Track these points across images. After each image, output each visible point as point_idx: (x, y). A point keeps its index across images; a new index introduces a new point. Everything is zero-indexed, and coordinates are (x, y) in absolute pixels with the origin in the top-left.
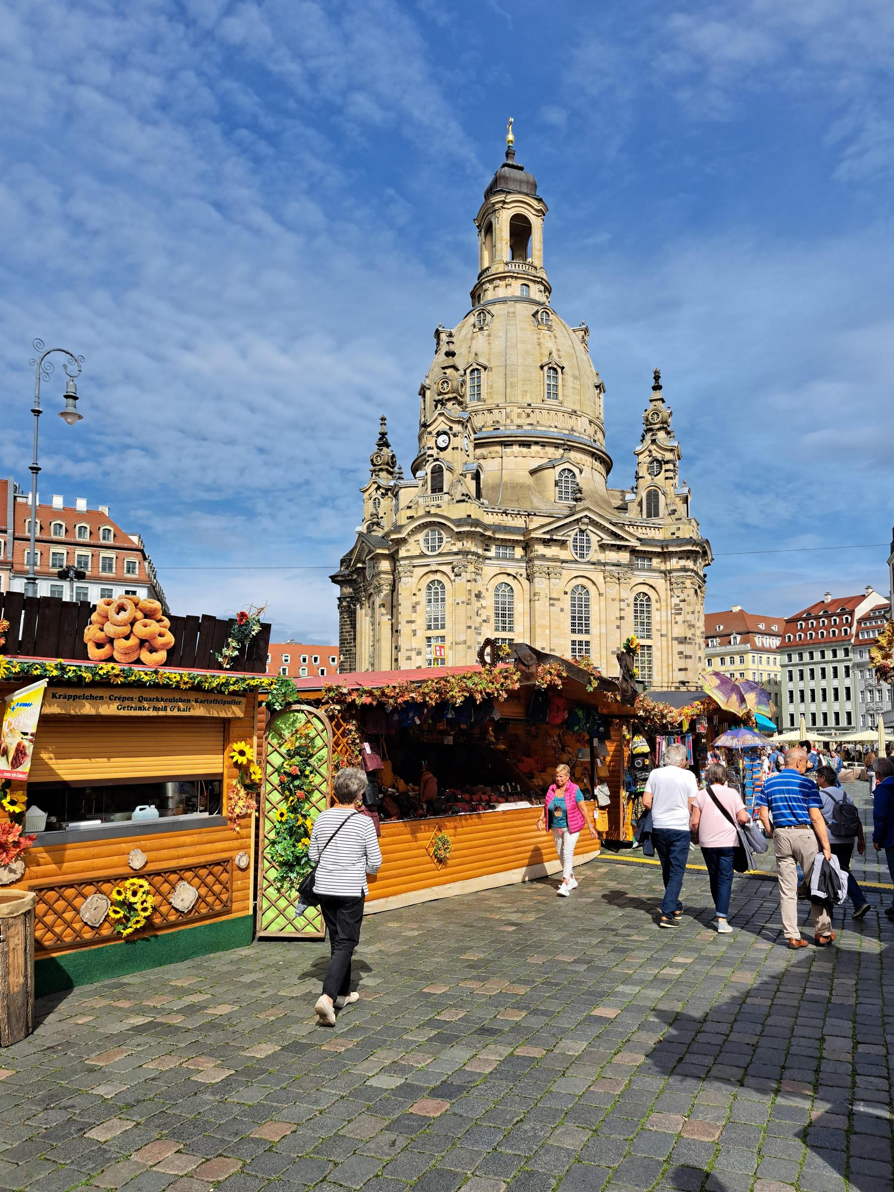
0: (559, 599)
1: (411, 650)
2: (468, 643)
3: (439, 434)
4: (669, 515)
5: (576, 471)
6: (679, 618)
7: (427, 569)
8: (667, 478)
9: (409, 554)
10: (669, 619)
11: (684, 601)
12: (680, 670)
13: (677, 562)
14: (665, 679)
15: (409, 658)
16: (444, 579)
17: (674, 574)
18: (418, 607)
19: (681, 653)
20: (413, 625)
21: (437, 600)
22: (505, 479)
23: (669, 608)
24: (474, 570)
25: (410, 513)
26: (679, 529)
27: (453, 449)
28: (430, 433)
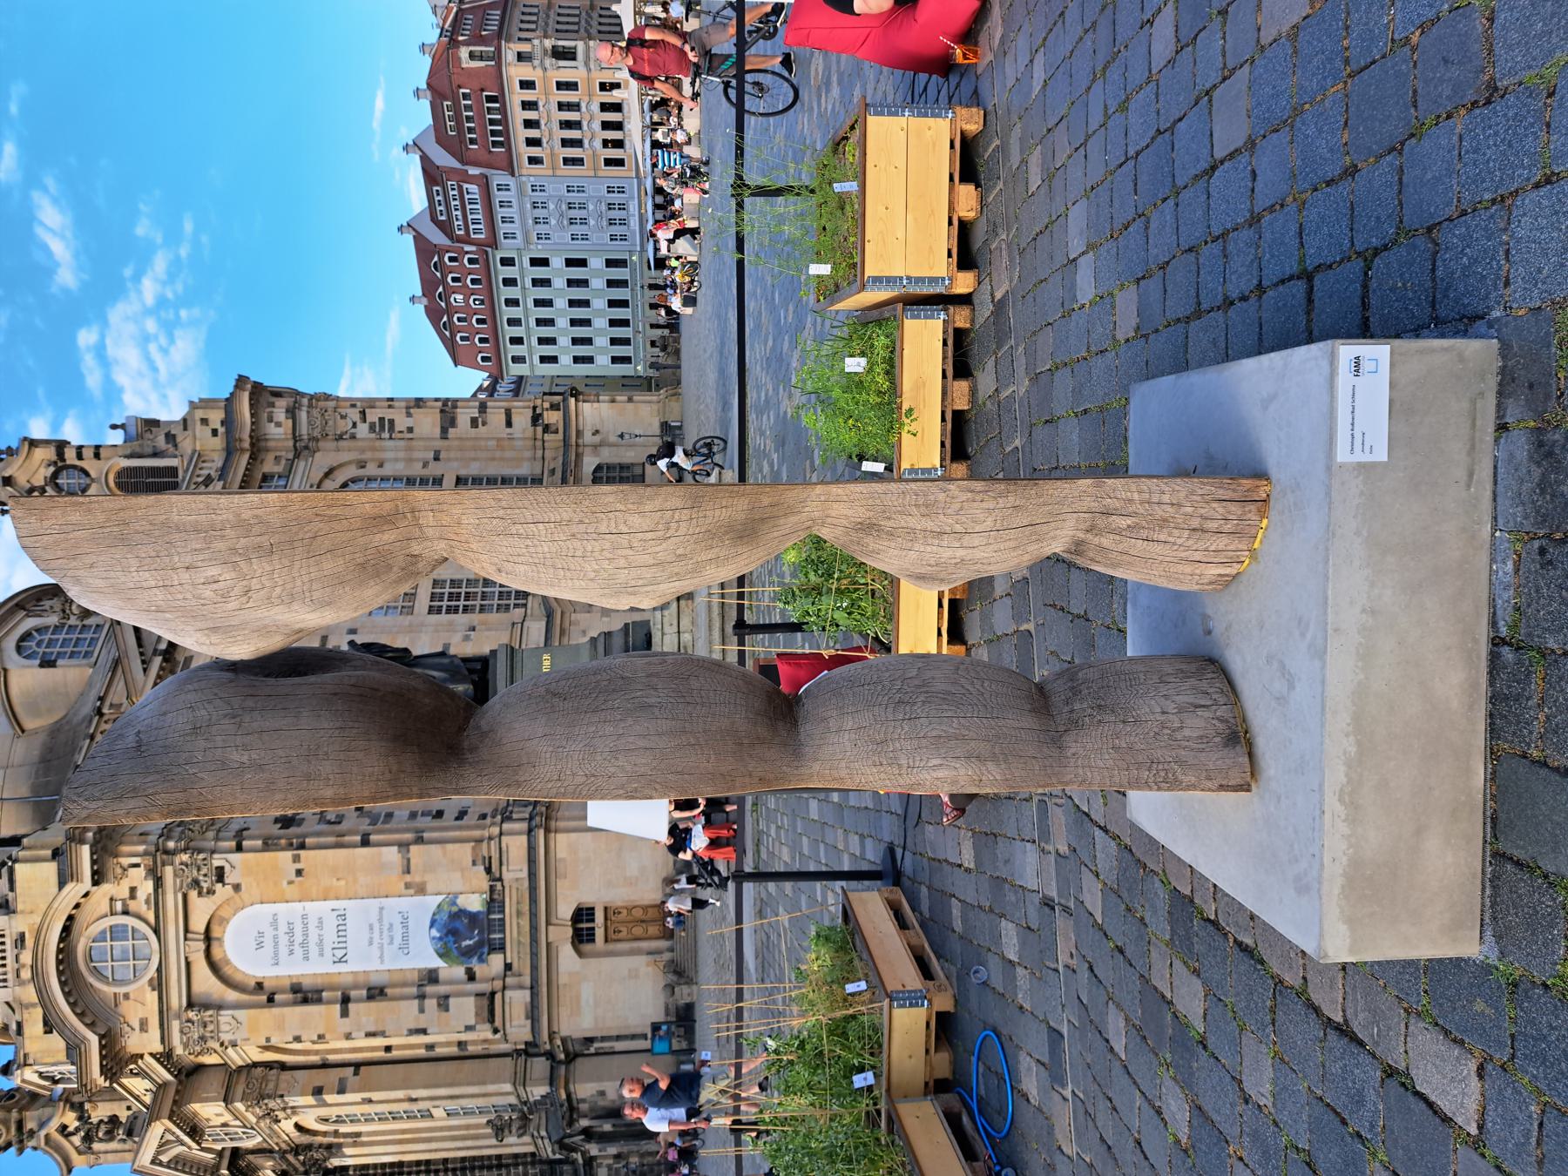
2: (409, 836)
4: (176, 446)
5: (30, 623)
6: (402, 423)
7: (201, 970)
8: (97, 456)
10: (402, 443)
11: (363, 413)
12: (509, 424)
13: (278, 425)
14: (528, 454)
15: (444, 1002)
17: (304, 430)
18: (307, 983)
20: (353, 994)
22: (24, 791)
23: (378, 443)
24: (211, 834)
25: (34, 1026)
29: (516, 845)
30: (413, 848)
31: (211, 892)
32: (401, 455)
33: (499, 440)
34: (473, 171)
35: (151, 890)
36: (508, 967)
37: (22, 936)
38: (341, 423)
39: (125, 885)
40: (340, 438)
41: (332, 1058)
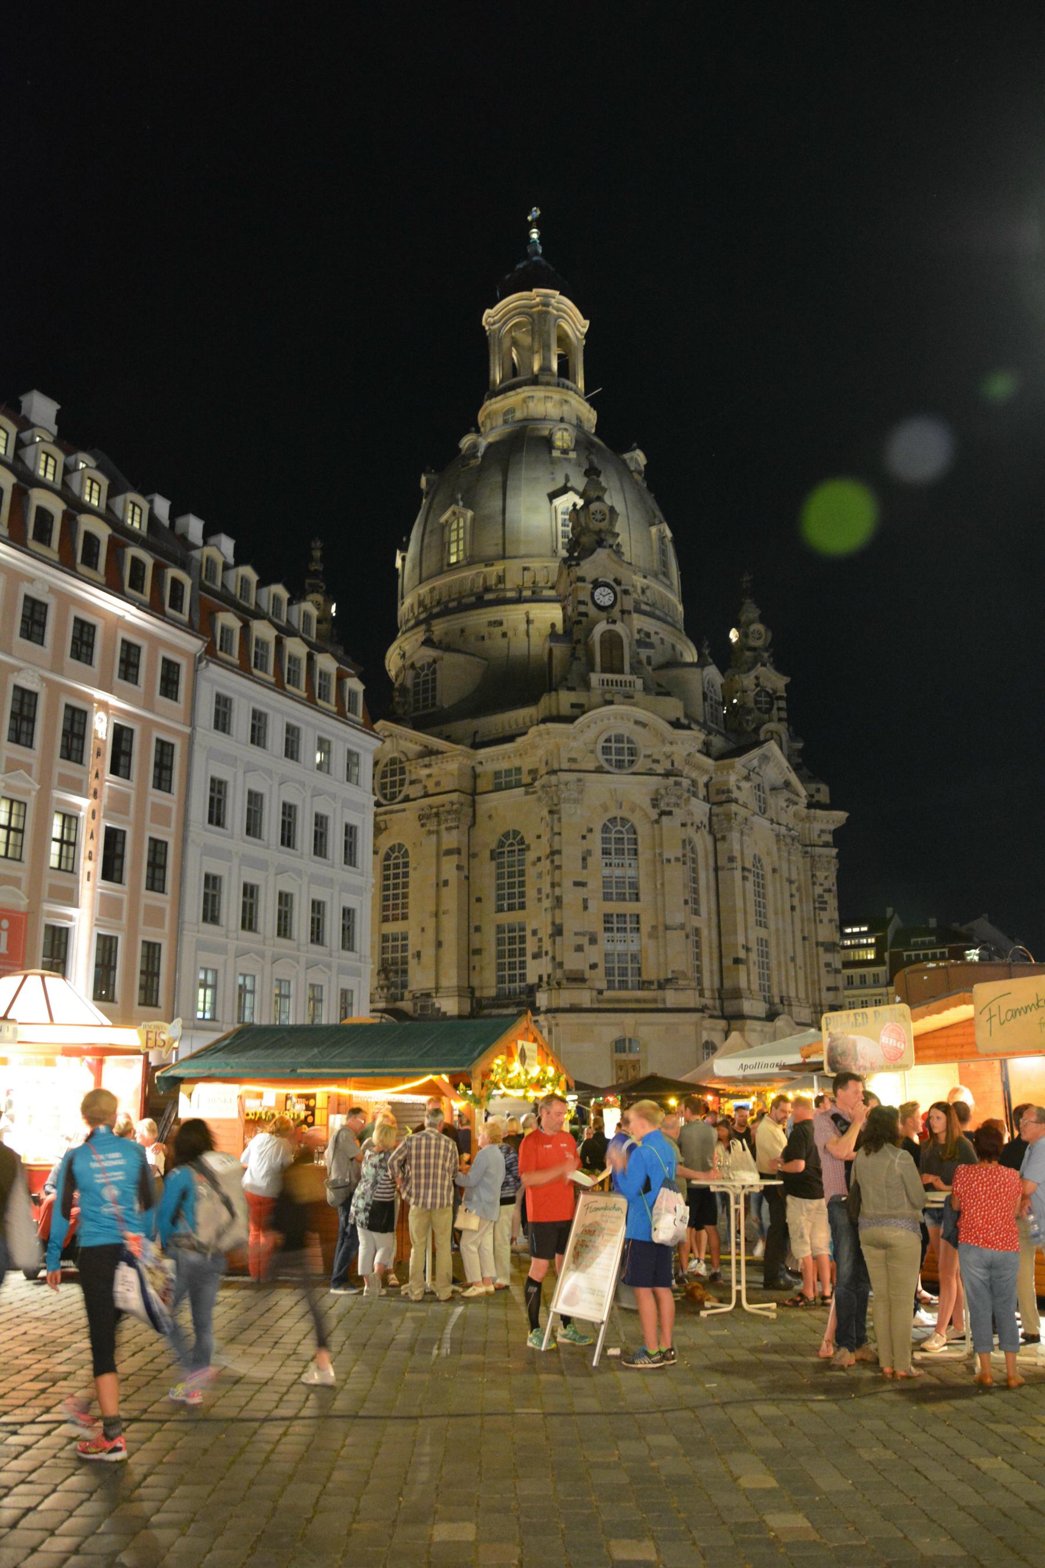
0: (749, 871)
1: (583, 934)
2: (688, 929)
3: (597, 584)
6: (825, 916)
9: (574, 766)
11: (830, 891)
12: (829, 989)
13: (819, 836)
15: (579, 948)
16: (636, 819)
18: (589, 859)
19: (828, 965)
20: (585, 889)
21: (620, 852)
26: (818, 790)
27: (623, 612)
28: (581, 579)
29: (689, 998)
30: (683, 933)
31: (654, 806)
32: (805, 914)
33: (819, 981)
34: (887, 955)
35: (659, 771)
36: (600, 992)
37: (632, 697)
38: (823, 878)
39: (662, 758)
40: (813, 876)
41: (474, 862)
